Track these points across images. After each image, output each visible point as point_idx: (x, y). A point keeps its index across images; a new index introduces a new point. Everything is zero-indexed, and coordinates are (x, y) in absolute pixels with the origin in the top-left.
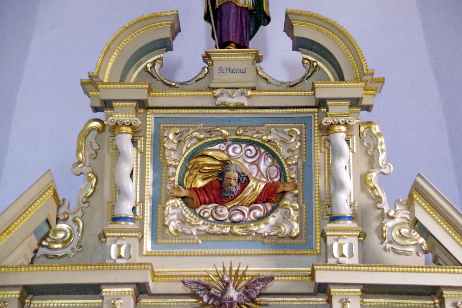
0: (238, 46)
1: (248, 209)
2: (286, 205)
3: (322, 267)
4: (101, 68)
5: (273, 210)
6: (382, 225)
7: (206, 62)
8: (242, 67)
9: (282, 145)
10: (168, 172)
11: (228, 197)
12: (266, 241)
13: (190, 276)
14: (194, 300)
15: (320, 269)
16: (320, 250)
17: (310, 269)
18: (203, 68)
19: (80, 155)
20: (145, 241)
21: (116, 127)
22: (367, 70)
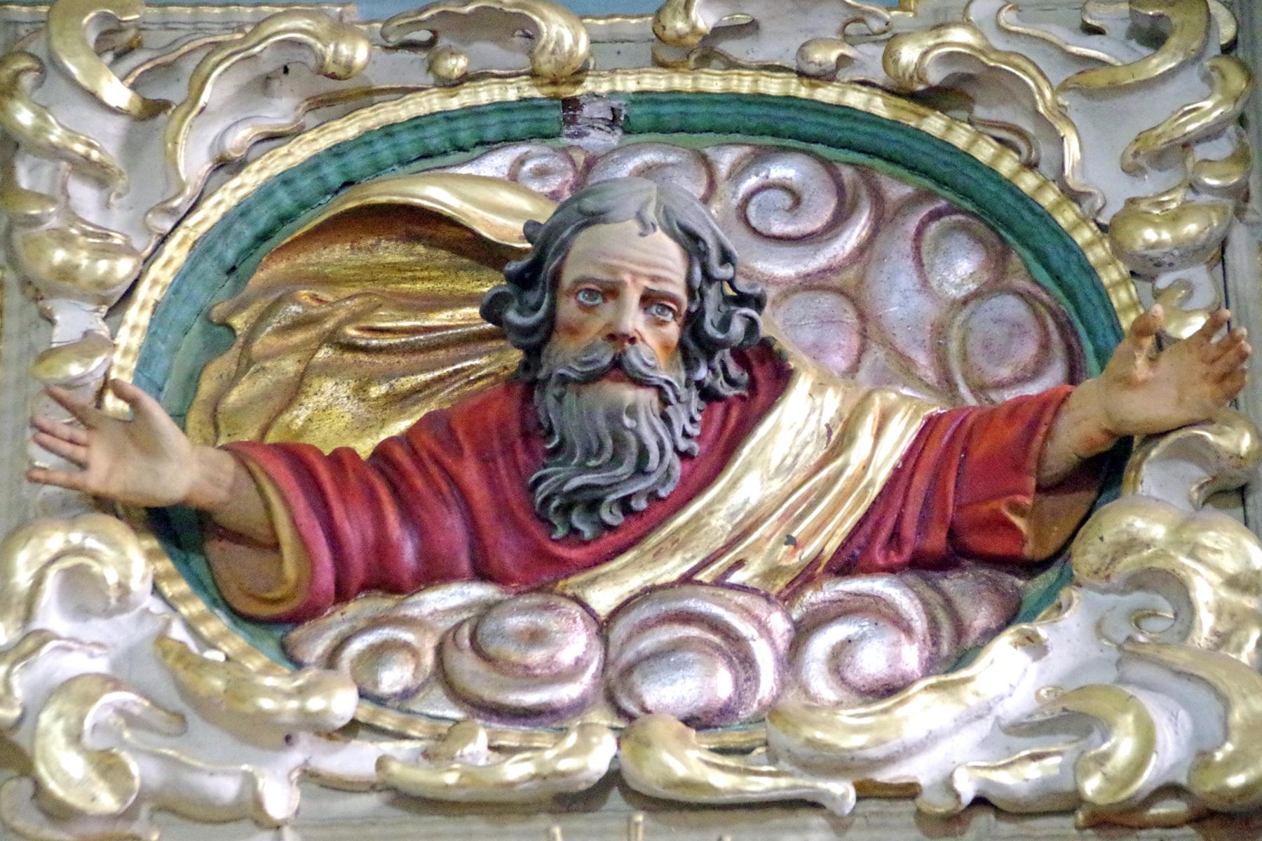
1: (779, 623)
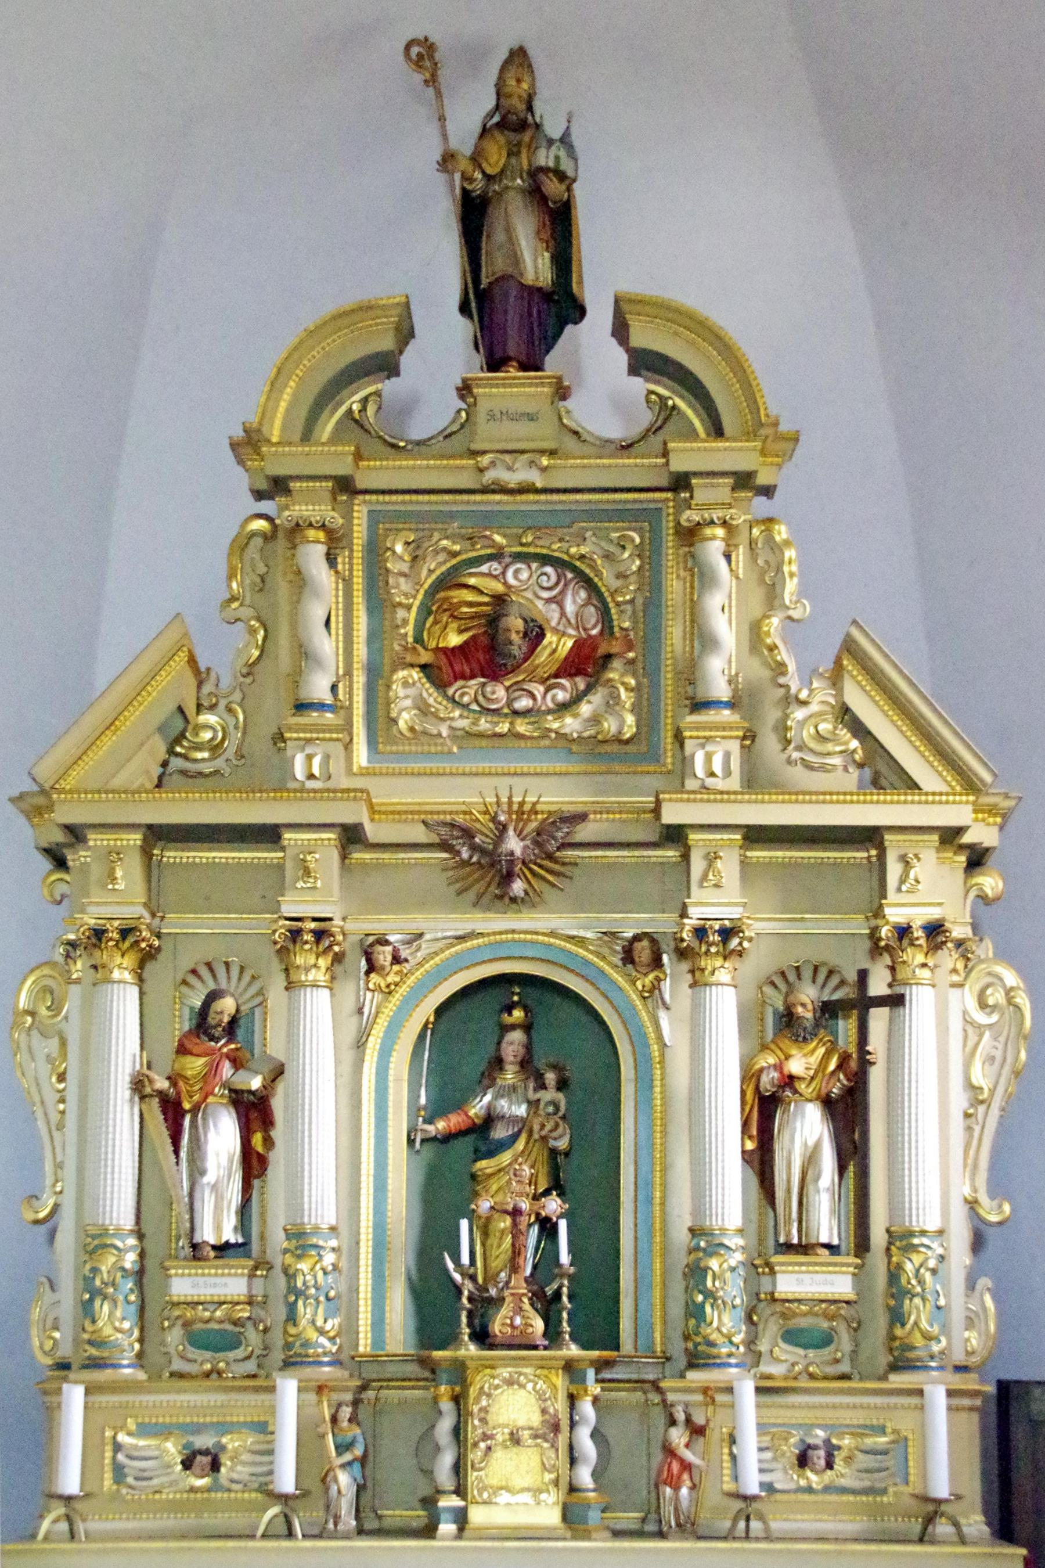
0: (524, 367)
1: (542, 689)
2: (610, 680)
3: (674, 796)
4: (266, 413)
5: (589, 689)
6: (786, 716)
7: (462, 398)
8: (531, 409)
9: (606, 565)
10: (394, 619)
11: (505, 665)
12: (575, 748)
13: (438, 813)
14: (445, 855)
15: (670, 800)
16: (673, 764)
17: (652, 799)
18: (459, 411)
19: (234, 585)
20: (355, 747)
21: (296, 530)
22: (767, 415)
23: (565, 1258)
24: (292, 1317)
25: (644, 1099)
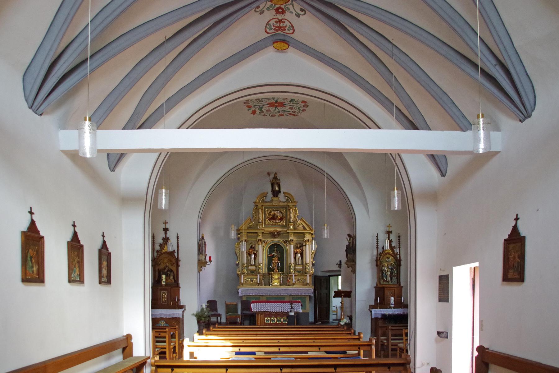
0: (276, 197)
23: (280, 265)
24: (258, 270)
25: (286, 253)
